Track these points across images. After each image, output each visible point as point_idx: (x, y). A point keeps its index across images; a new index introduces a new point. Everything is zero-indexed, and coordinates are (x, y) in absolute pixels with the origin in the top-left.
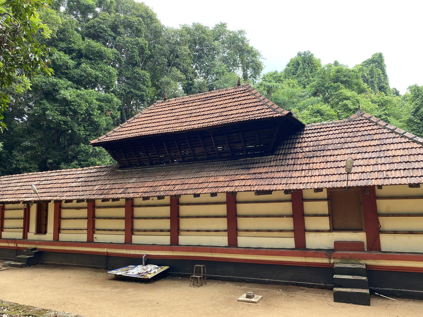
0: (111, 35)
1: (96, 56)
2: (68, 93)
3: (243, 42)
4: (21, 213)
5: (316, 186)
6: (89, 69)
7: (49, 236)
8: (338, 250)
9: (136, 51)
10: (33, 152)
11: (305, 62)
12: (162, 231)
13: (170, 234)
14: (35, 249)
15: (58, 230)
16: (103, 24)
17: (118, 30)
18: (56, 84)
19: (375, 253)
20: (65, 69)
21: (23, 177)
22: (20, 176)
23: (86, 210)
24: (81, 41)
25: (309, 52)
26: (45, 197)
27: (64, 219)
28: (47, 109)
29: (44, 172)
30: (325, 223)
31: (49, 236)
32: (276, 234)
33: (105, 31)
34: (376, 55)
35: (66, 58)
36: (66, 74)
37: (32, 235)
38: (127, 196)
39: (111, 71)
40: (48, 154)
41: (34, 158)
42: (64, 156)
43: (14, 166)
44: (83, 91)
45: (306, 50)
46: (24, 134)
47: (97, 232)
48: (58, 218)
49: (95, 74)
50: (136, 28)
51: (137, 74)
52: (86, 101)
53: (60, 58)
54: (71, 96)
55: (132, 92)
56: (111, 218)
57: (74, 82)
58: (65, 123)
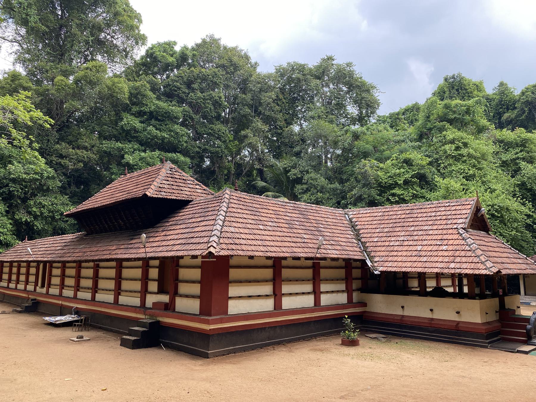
0: (184, 93)
1: (165, 117)
11: (453, 88)
12: (103, 290)
13: (140, 296)
17: (193, 86)
19: (169, 313)
33: (179, 88)
36: (137, 137)
47: (65, 288)
53: (128, 124)
57: (142, 145)
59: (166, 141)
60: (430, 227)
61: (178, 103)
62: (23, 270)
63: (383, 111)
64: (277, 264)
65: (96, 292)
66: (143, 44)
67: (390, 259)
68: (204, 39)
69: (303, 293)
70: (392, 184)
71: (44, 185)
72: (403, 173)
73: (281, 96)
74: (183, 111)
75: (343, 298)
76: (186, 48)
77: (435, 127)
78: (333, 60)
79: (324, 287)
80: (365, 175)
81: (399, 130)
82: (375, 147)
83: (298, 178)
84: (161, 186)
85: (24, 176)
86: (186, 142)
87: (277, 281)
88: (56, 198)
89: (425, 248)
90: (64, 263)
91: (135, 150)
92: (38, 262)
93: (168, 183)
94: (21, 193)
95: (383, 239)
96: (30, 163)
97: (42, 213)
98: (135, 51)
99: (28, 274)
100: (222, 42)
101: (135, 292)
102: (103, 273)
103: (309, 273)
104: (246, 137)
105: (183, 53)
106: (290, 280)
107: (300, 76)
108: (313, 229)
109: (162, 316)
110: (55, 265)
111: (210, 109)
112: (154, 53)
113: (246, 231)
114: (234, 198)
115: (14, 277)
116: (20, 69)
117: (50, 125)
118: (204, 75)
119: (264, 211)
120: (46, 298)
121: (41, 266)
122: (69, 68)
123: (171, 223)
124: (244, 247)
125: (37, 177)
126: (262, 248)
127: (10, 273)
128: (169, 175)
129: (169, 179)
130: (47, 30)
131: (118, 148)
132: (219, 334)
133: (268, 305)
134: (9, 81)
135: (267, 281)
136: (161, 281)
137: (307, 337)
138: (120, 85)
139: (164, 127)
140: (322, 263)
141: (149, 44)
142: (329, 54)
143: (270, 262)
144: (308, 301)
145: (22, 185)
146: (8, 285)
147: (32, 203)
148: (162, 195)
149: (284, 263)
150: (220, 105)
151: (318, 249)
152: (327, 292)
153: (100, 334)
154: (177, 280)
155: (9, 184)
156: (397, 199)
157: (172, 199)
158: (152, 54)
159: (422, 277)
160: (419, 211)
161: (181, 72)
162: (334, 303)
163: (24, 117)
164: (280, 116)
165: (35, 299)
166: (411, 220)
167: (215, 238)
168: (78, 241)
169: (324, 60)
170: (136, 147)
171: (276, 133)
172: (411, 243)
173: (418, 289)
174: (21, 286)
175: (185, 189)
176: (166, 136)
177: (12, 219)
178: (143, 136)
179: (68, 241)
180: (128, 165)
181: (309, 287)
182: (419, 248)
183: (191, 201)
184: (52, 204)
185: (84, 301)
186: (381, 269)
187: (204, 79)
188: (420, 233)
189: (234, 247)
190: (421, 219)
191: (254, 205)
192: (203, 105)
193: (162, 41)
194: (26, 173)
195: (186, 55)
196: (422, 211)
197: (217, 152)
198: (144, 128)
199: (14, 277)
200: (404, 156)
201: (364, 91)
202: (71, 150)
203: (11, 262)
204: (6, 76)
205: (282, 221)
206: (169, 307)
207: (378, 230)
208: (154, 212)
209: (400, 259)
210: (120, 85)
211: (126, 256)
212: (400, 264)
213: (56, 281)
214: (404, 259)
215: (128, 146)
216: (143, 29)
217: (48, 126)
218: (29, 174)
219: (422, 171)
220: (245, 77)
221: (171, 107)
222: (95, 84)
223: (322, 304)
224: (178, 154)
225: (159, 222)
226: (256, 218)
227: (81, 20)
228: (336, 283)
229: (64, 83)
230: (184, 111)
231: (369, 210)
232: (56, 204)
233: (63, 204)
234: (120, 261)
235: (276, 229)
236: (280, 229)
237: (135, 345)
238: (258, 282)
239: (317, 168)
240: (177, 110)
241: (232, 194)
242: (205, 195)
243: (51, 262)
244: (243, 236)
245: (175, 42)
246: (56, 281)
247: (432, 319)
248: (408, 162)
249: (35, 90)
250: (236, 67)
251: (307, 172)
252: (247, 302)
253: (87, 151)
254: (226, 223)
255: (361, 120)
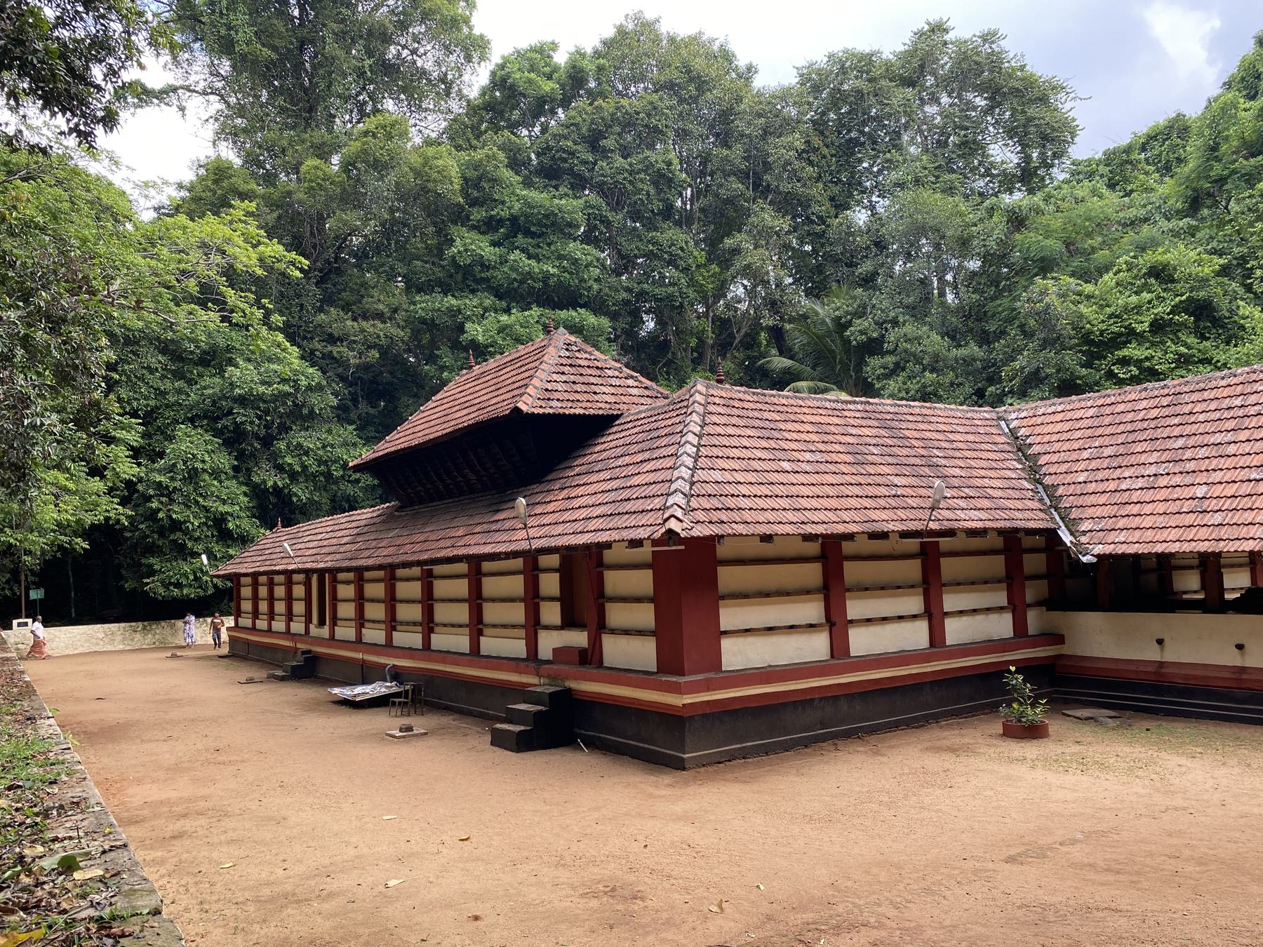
0: (585, 162)
1: (546, 226)
6: (526, 263)
8: (561, 663)
12: (445, 625)
20: (480, 272)
23: (466, 581)
33: (572, 154)
36: (487, 280)
47: (367, 625)
53: (466, 250)
57: (500, 297)
59: (552, 281)
60: (1230, 437)
61: (572, 188)
62: (280, 591)
63: (1088, 146)
64: (831, 552)
65: (431, 630)
66: (482, 58)
67: (1121, 523)
68: (621, 25)
69: (901, 618)
70: (1121, 335)
71: (303, 405)
72: (1149, 302)
73: (817, 142)
74: (586, 207)
75: (1002, 626)
76: (580, 54)
77: (1234, 172)
78: (946, 31)
79: (950, 602)
80: (1045, 318)
81: (1132, 191)
82: (1068, 244)
83: (871, 340)
84: (549, 386)
85: (262, 389)
86: (597, 280)
87: (832, 590)
88: (329, 431)
89: (1217, 491)
90: (359, 571)
91: (486, 310)
92: (308, 572)
93: (564, 378)
94: (259, 426)
95: (1100, 475)
96: (272, 362)
97: (305, 467)
98: (466, 77)
99: (289, 599)
100: (665, 28)
101: (514, 626)
102: (441, 588)
103: (912, 569)
104: (736, 251)
105: (574, 67)
106: (865, 589)
107: (861, 84)
108: (918, 461)
109: (575, 679)
110: (341, 576)
111: (648, 194)
112: (508, 76)
113: (751, 477)
114: (717, 400)
115: (263, 606)
116: (230, 154)
117: (302, 270)
118: (627, 113)
119: (790, 426)
120: (329, 647)
121: (315, 579)
122: (327, 137)
123: (577, 470)
124: (747, 516)
125: (286, 388)
126: (791, 516)
127: (255, 599)
128: (564, 361)
129: (566, 369)
130: (274, 56)
131: (450, 309)
132: (705, 716)
133: (816, 647)
134: (210, 183)
135: (808, 592)
136: (567, 599)
137: (915, 719)
138: (440, 162)
139: (545, 251)
140: (945, 543)
141: (496, 58)
142: (934, 17)
143: (814, 548)
144: (916, 635)
145: (259, 408)
146: (254, 624)
147: (282, 445)
148: (554, 408)
149: (847, 547)
150: (670, 180)
151: (933, 509)
152: (961, 613)
153: (446, 720)
154: (601, 598)
155: (232, 409)
156: (1135, 371)
157: (575, 415)
158: (504, 80)
159: (1210, 565)
160: (1195, 397)
161: (573, 113)
162: (980, 637)
163: (246, 259)
164: (816, 191)
165: (309, 652)
166: (1176, 421)
167: (679, 499)
168: (383, 521)
169: (920, 34)
170: (487, 302)
171: (809, 234)
172: (1177, 480)
173: (1201, 596)
174: (279, 625)
175: (604, 389)
176: (552, 271)
177: (246, 484)
178: (499, 275)
179: (363, 523)
180: (474, 344)
181: (914, 603)
182: (1200, 491)
183: (618, 417)
184: (324, 447)
185: (408, 652)
186: (1099, 549)
187: (628, 123)
188: (1203, 452)
189: (723, 516)
190: (1202, 417)
191: (766, 415)
192: (630, 187)
193: (524, 45)
194: (263, 383)
195: (582, 70)
196: (1206, 395)
197: (670, 297)
198: (501, 256)
199: (263, 606)
200: (1149, 258)
201: (1031, 101)
202: (349, 323)
203: (255, 576)
204: (202, 171)
205: (838, 447)
206: (589, 658)
207: (1085, 454)
208: (537, 449)
209: (1148, 522)
210: (440, 162)
211: (488, 549)
212: (1149, 535)
213: (346, 610)
214: (1161, 521)
215: (470, 303)
216: (481, 23)
217: (298, 274)
218: (269, 384)
219: (1202, 294)
220: (725, 106)
221: (556, 201)
222: (385, 166)
223: (951, 639)
224: (582, 311)
225: (552, 471)
226: (773, 444)
227: (343, 21)
228: (984, 591)
229: (320, 173)
230: (588, 205)
231: (1060, 404)
232: (332, 446)
233: (345, 444)
234: (475, 562)
235: (823, 467)
236: (832, 468)
237: (523, 744)
238: (788, 594)
239: (918, 311)
240: (571, 205)
241: (712, 392)
242: (649, 401)
243: (333, 571)
244: (744, 490)
245: (553, 43)
246: (346, 610)
247: (1243, 670)
248: (1161, 274)
249: (263, 197)
250: (702, 84)
251: (895, 323)
252: (765, 643)
253: (385, 322)
254: (702, 462)
255: (1028, 176)
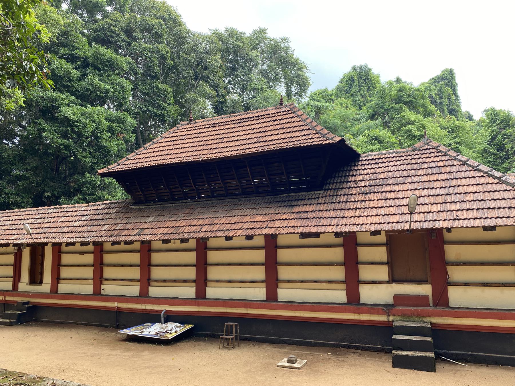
0: (124, 41)
1: (106, 66)
2: (71, 111)
3: (286, 52)
4: (10, 259)
5: (373, 228)
7: (46, 287)
8: (399, 306)
9: (156, 60)
10: (26, 183)
11: (361, 78)
12: (185, 281)
14: (28, 303)
15: (56, 279)
16: (115, 26)
17: (134, 34)
18: (56, 100)
19: (442, 309)
20: (67, 81)
21: (13, 214)
22: (9, 212)
23: (92, 255)
24: (87, 47)
25: (366, 66)
26: (41, 239)
27: (65, 266)
28: (44, 131)
29: (40, 208)
30: (382, 273)
31: (46, 287)
32: (324, 285)
33: (118, 35)
34: (446, 71)
35: (69, 67)
36: (68, 87)
37: (24, 286)
38: (142, 238)
39: (124, 84)
40: (45, 185)
41: (27, 190)
42: (65, 188)
43: (3, 200)
44: (89, 109)
45: (363, 64)
46: (15, 160)
47: (105, 282)
48: (57, 265)
49: (105, 88)
50: (156, 32)
51: (157, 88)
52: (94, 121)
54: (74, 115)
55: (149, 111)
56: (122, 266)
57: (78, 97)
58: (67, 147)
142: (263, 27)
